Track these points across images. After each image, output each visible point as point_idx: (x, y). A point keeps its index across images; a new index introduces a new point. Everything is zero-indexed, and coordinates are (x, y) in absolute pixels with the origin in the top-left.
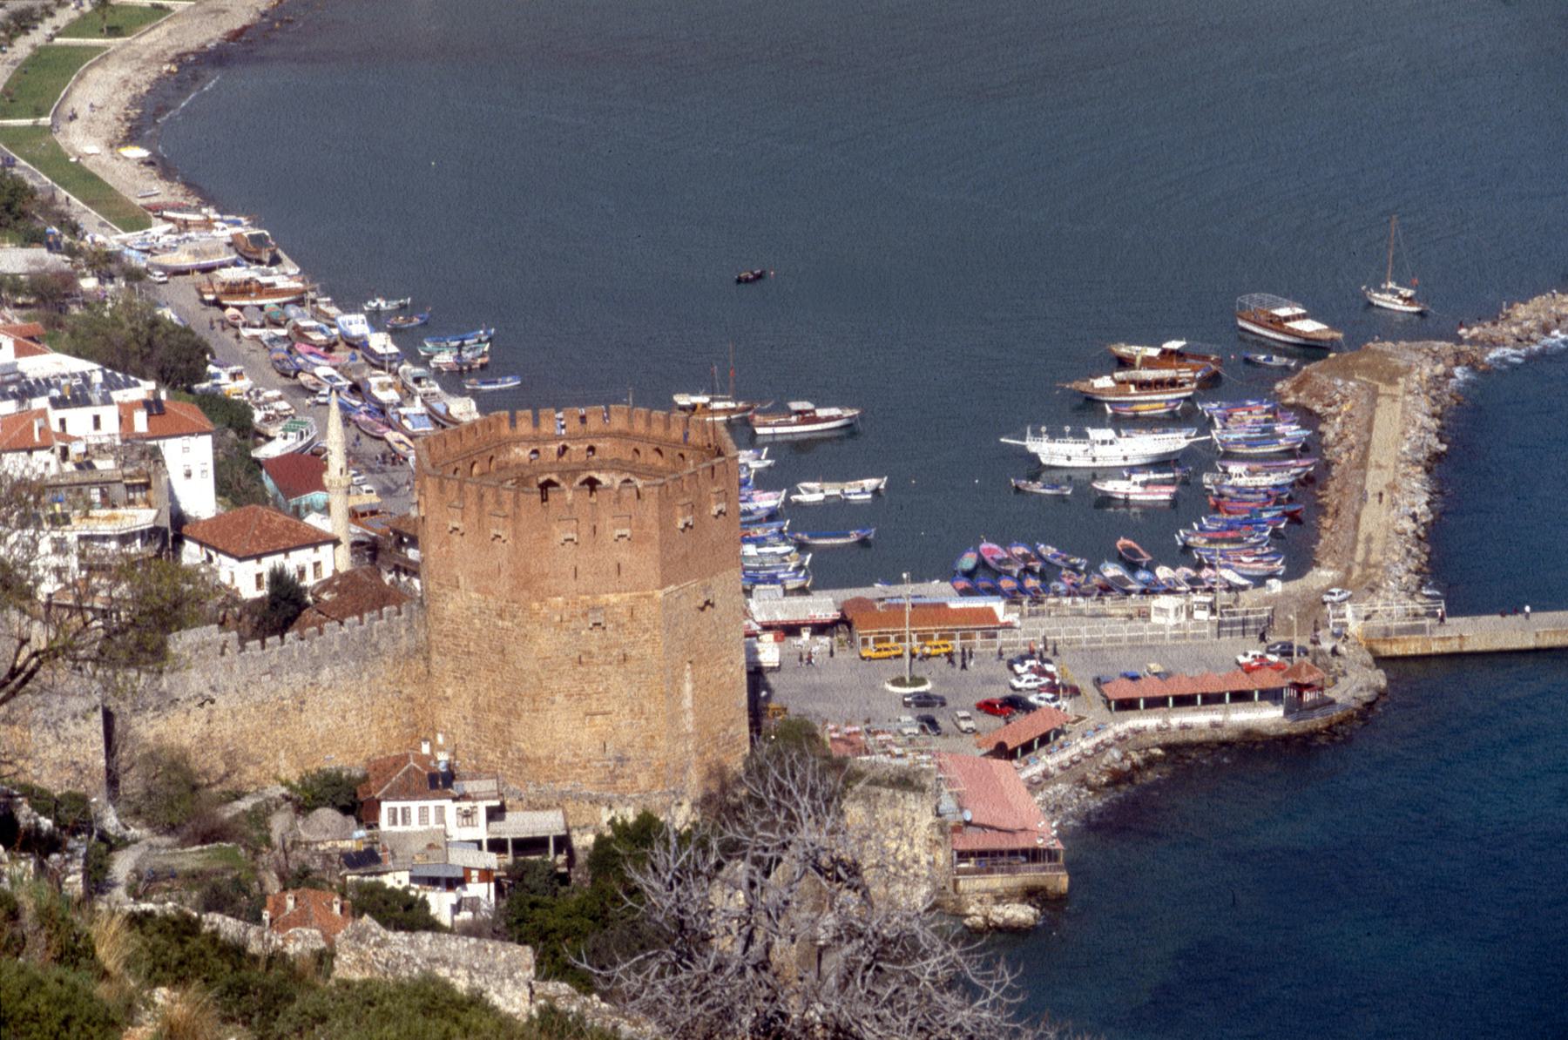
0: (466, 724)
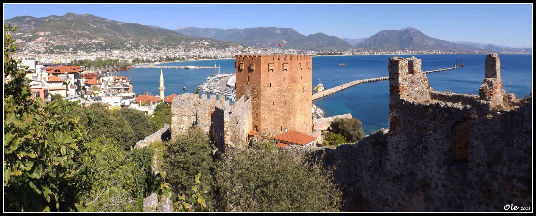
0: (272, 125)
